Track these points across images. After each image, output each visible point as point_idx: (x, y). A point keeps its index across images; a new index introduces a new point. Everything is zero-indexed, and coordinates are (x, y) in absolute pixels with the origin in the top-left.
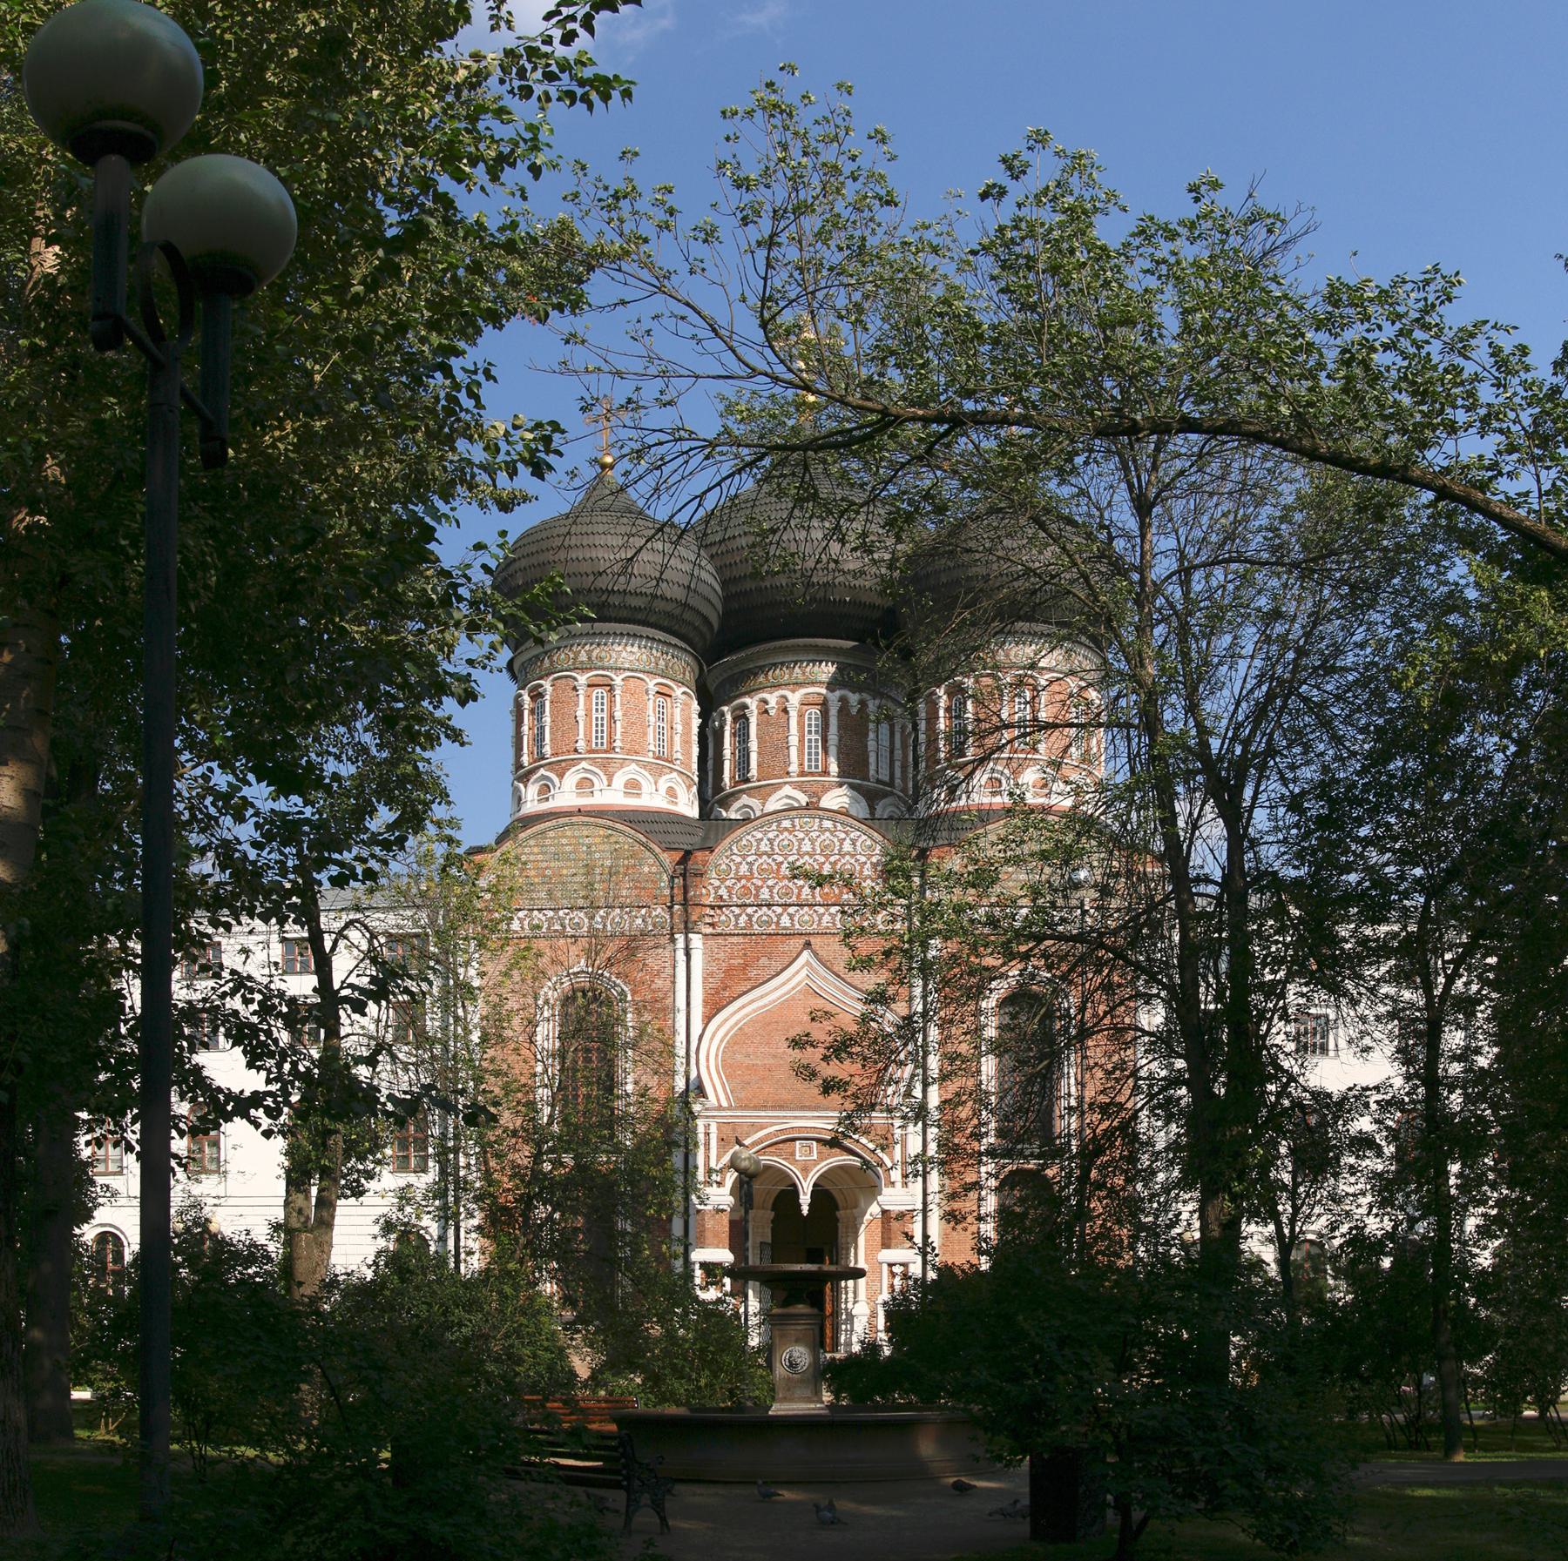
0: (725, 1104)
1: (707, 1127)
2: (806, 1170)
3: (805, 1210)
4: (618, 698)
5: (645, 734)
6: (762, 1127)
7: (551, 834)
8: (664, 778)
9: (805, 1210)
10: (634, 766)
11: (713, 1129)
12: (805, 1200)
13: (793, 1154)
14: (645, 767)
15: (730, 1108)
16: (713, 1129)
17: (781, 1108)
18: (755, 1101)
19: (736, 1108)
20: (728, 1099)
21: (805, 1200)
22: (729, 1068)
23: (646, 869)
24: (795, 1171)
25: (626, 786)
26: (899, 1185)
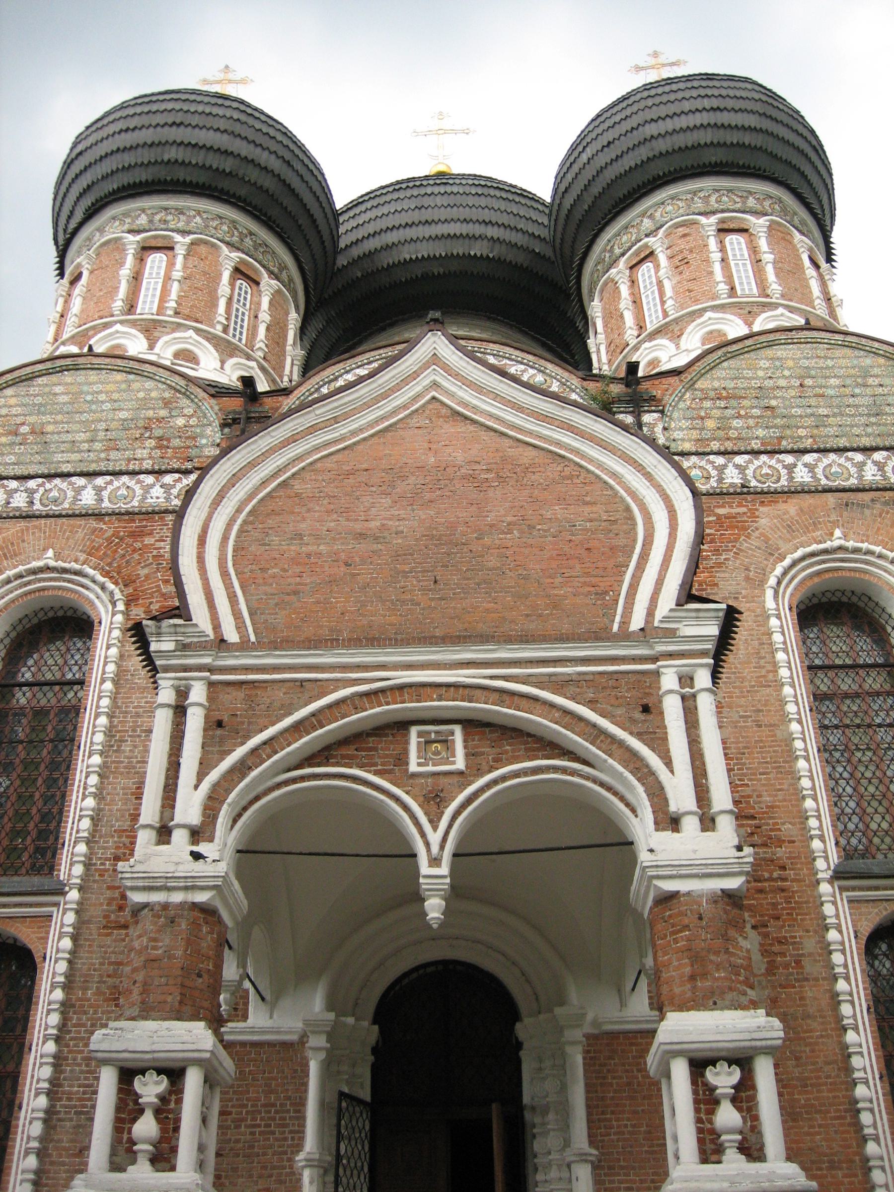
0: (232, 636)
1: (182, 694)
2: (434, 801)
3: (434, 908)
4: (180, 260)
5: (214, 305)
6: (323, 688)
7: (40, 381)
8: (234, 360)
9: (434, 908)
10: (191, 333)
11: (198, 693)
12: (434, 873)
13: (402, 760)
14: (208, 339)
15: (244, 646)
16: (198, 693)
17: (373, 641)
18: (308, 631)
19: (259, 646)
20: (240, 626)
21: (434, 873)
22: (249, 556)
23: (180, 422)
24: (405, 809)
25: (177, 355)
26: (691, 824)
